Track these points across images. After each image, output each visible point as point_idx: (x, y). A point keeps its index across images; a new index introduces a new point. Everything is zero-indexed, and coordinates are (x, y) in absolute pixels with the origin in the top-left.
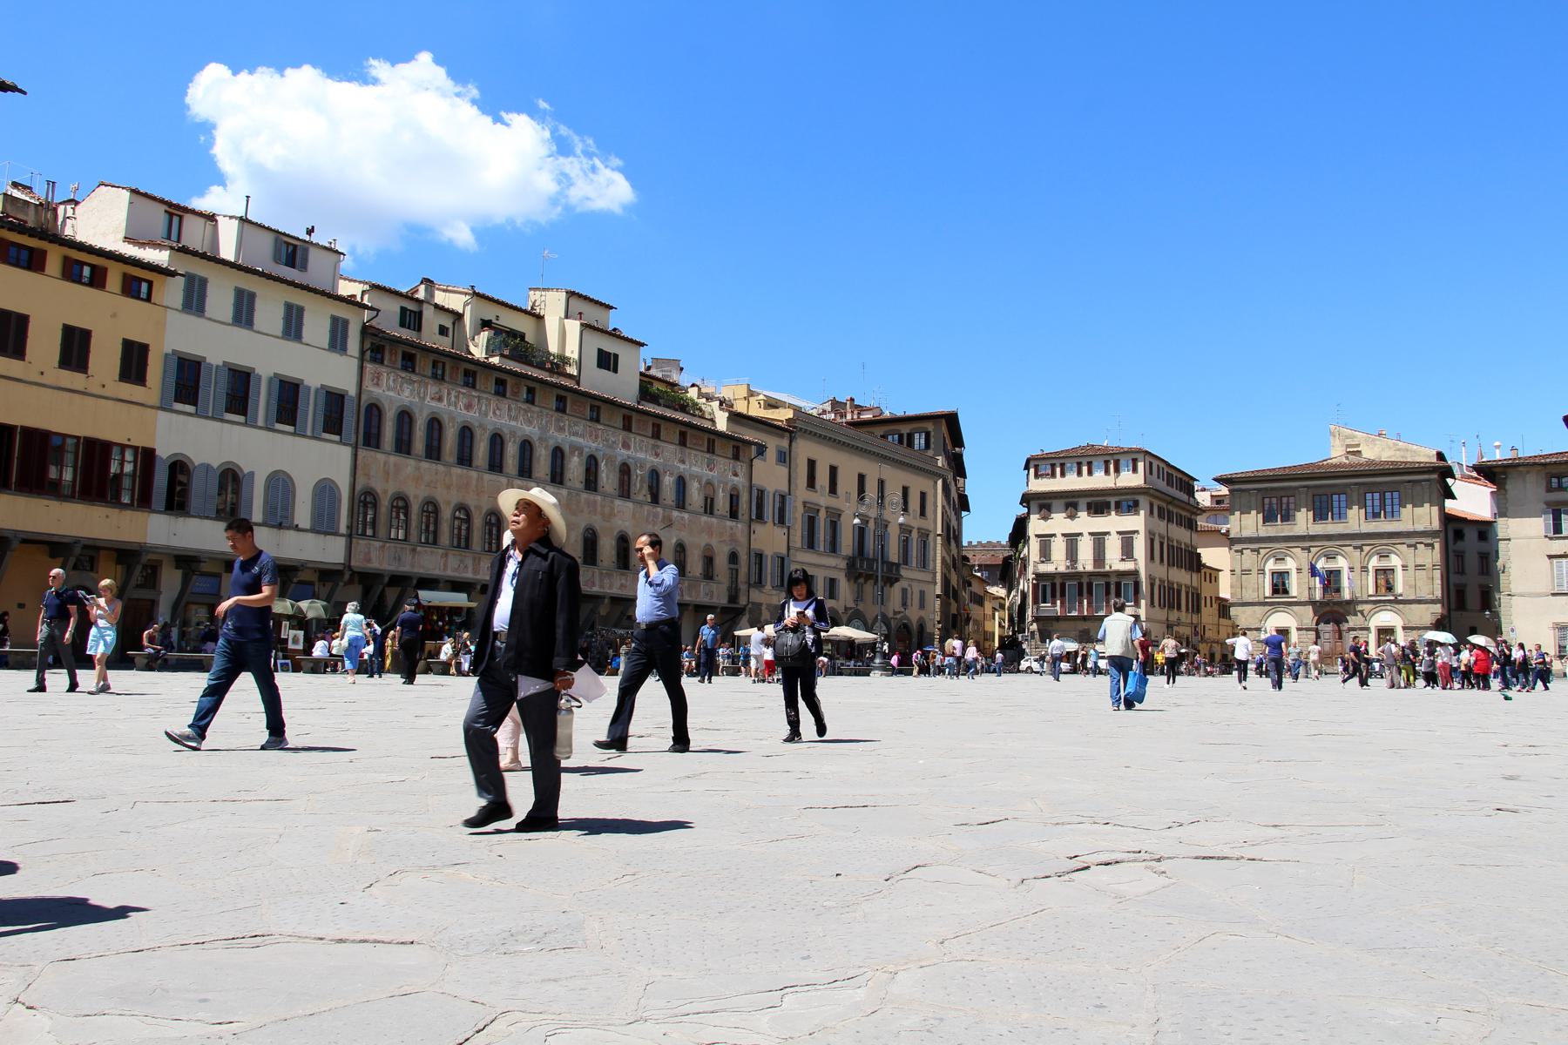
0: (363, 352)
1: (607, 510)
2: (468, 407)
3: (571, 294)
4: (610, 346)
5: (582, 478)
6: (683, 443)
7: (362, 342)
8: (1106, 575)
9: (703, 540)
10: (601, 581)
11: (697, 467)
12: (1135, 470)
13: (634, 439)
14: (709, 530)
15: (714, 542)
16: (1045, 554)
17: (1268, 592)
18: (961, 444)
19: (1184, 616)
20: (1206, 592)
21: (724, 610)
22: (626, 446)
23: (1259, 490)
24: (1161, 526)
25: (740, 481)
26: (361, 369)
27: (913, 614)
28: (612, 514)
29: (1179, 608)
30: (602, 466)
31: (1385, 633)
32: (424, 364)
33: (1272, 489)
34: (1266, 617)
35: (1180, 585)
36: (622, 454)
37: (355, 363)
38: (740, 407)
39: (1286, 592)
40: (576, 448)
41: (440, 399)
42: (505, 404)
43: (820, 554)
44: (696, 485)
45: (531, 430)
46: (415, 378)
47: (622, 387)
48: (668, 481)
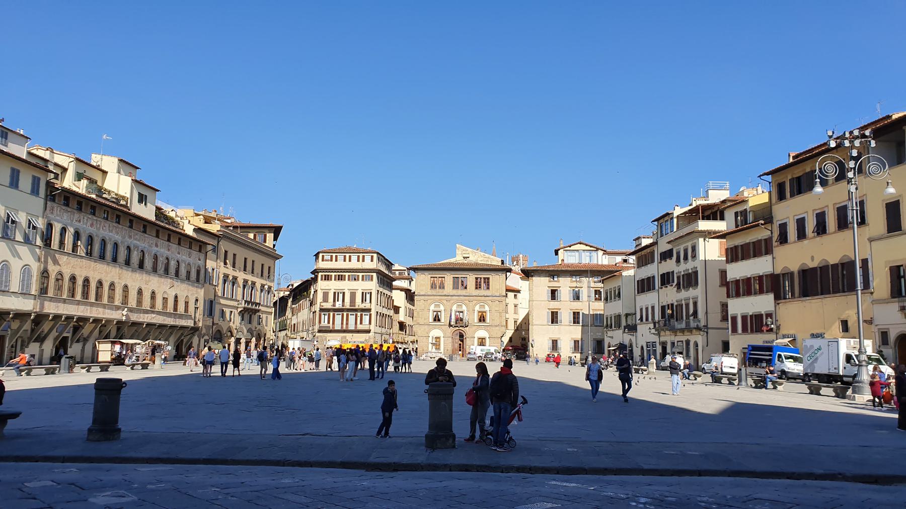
0: (47, 196)
2: (92, 225)
3: (121, 161)
4: (144, 192)
5: (138, 262)
6: (179, 244)
7: (46, 190)
8: (356, 310)
11: (186, 257)
12: (372, 261)
13: (160, 242)
16: (325, 299)
17: (431, 320)
20: (395, 317)
21: (192, 328)
22: (157, 246)
25: (201, 263)
26: (46, 204)
30: (146, 256)
31: (482, 342)
32: (74, 203)
36: (154, 249)
37: (42, 201)
39: (439, 320)
40: (137, 247)
41: (80, 221)
42: (107, 224)
45: (118, 238)
46: (69, 209)
47: (147, 212)
48: (173, 264)
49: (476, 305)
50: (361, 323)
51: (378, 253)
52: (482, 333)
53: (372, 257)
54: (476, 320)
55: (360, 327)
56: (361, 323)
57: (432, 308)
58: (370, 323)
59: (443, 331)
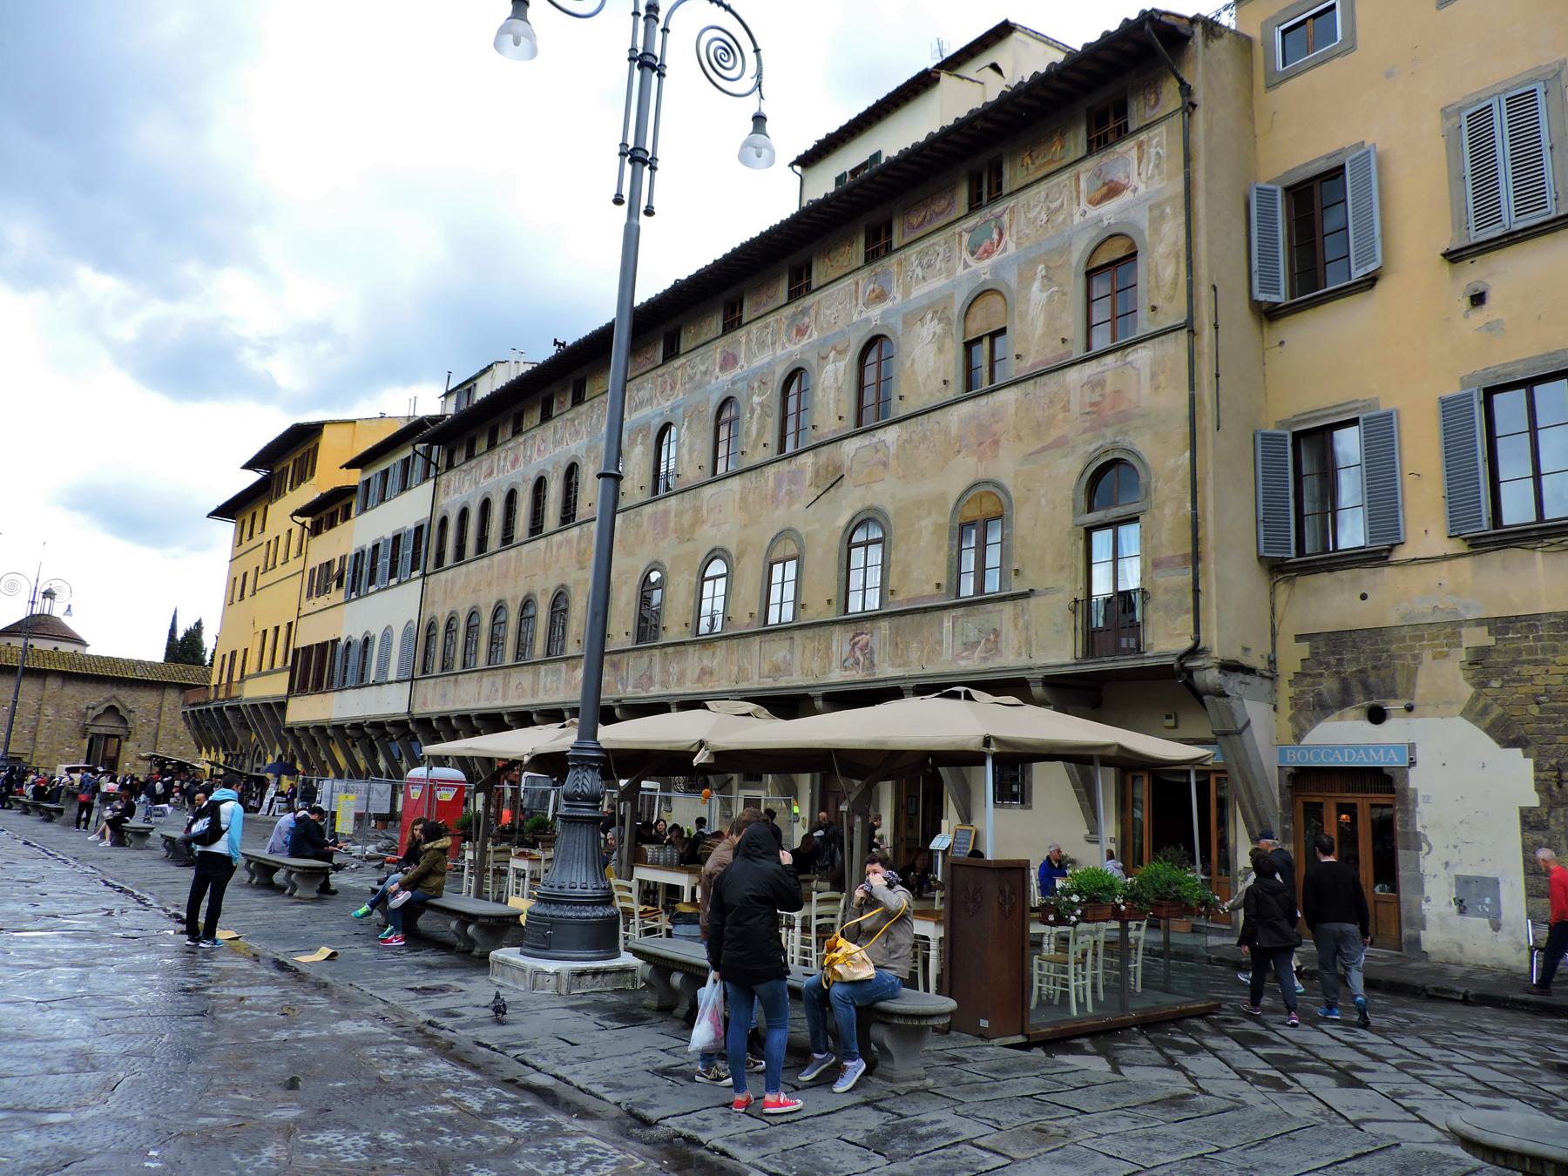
1: (687, 519)
10: (665, 671)
15: (1005, 468)
28: (697, 522)
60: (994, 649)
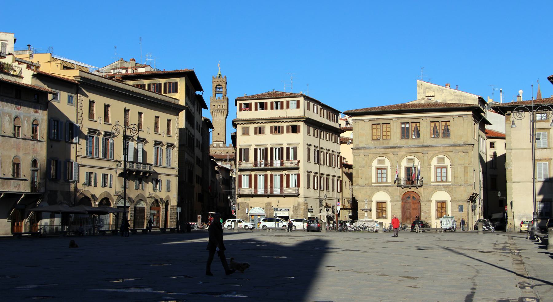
9: (13, 153)
12: (298, 107)
14: (18, 149)
15: (21, 154)
18: (201, 89)
19: (330, 194)
23: (370, 120)
24: (315, 141)
27: (162, 195)
29: (327, 189)
31: (441, 207)
33: (377, 119)
34: (372, 194)
35: (328, 175)
38: (45, 69)
43: (97, 159)
44: (7, 118)
49: (432, 158)
50: (288, 186)
51: (307, 98)
52: (442, 195)
53: (298, 102)
54: (433, 179)
55: (287, 191)
56: (288, 186)
57: (375, 164)
58: (298, 185)
59: (390, 194)
60: (19, 188)
